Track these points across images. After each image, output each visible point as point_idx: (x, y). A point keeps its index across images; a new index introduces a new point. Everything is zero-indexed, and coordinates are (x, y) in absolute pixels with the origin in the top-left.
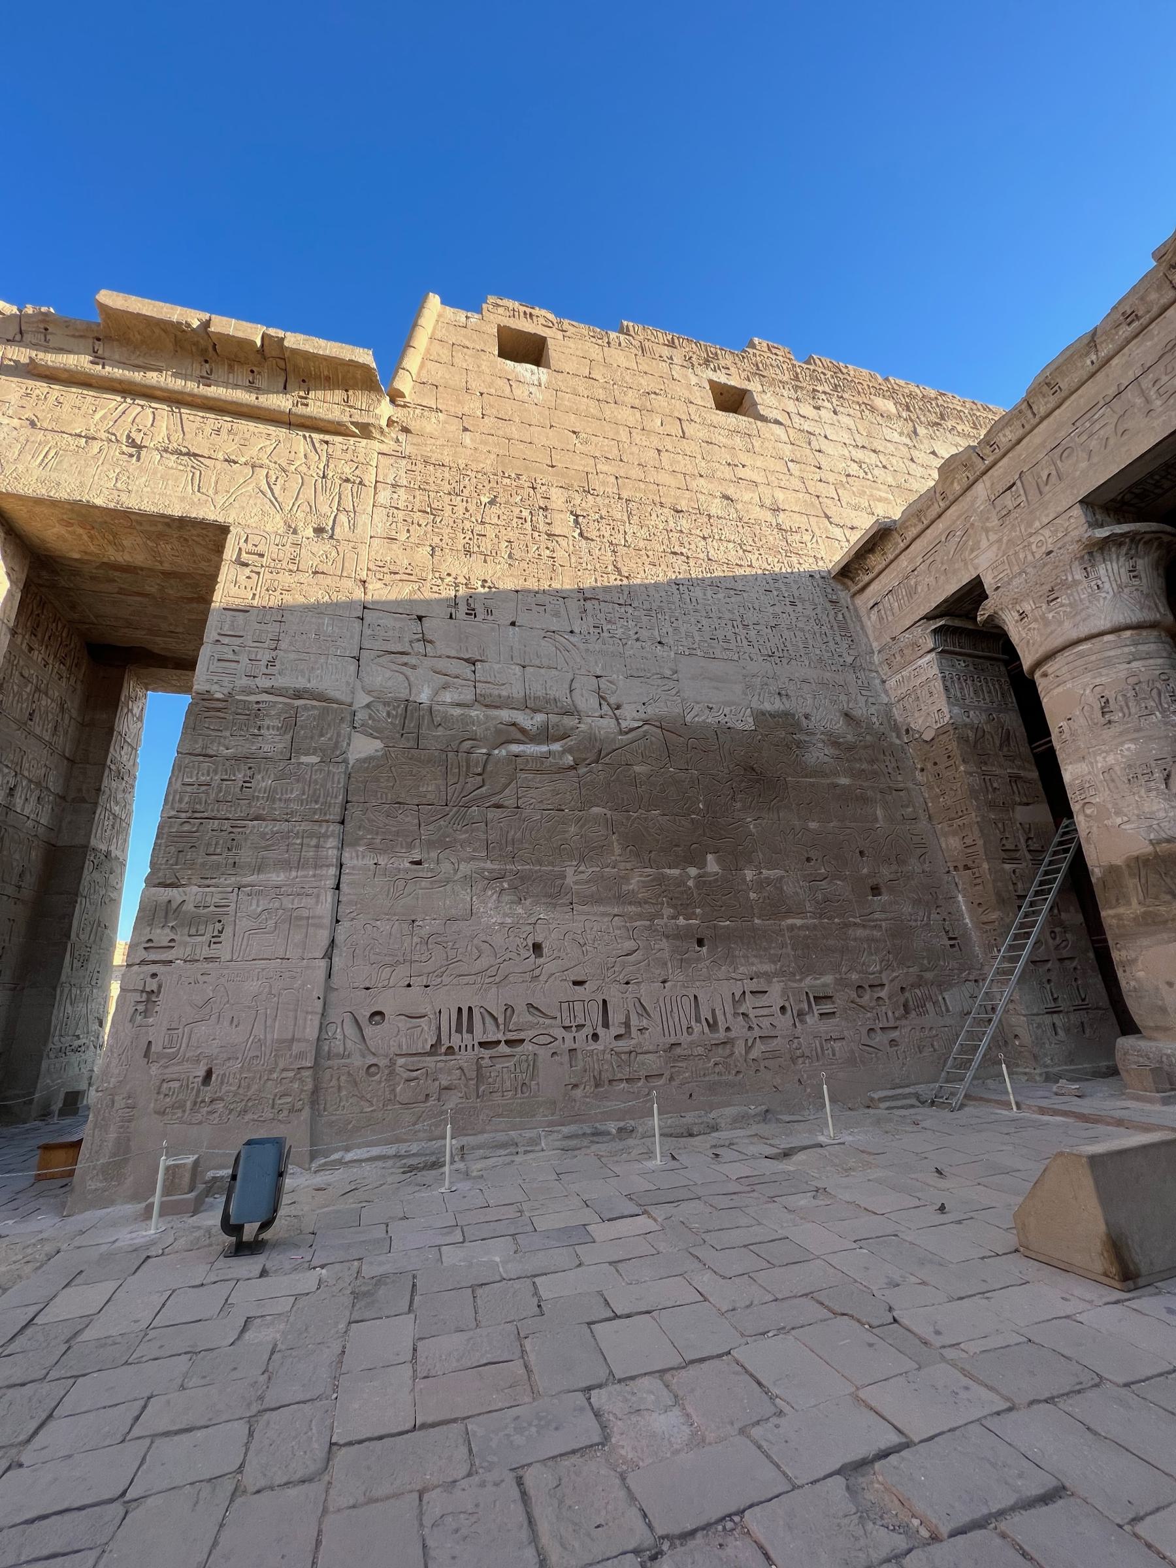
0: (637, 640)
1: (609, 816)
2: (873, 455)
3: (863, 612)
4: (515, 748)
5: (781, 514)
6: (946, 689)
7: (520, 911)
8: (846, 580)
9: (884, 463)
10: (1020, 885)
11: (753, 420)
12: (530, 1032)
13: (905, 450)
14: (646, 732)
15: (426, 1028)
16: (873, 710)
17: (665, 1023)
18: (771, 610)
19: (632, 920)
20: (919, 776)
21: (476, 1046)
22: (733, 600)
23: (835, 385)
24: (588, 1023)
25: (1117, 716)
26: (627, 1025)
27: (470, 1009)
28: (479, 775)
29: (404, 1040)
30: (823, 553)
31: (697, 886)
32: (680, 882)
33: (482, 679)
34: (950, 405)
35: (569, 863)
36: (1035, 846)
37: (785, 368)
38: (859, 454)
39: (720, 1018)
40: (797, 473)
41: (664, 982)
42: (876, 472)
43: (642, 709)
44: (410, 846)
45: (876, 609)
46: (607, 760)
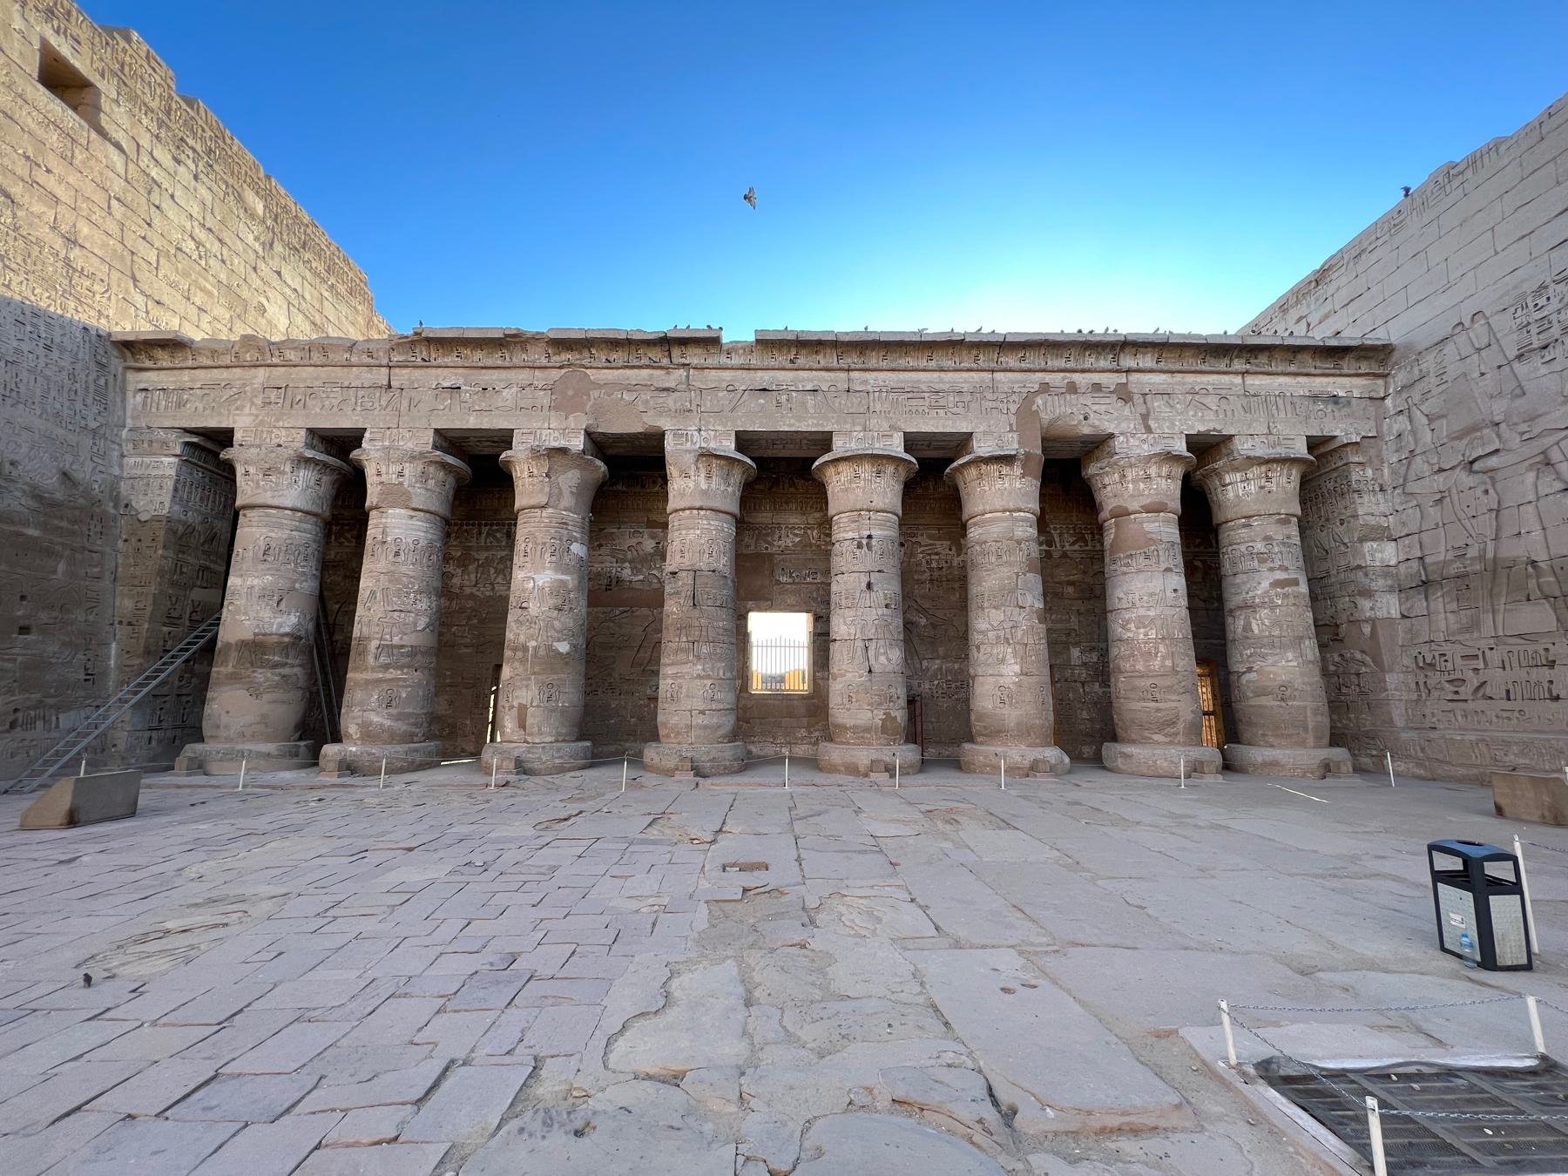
2: (217, 244)
3: (131, 387)
5: (77, 250)
6: (176, 490)
8: (126, 351)
9: (225, 258)
10: (170, 642)
11: (86, 125)
13: (253, 256)
16: (99, 477)
18: (15, 344)
20: (120, 543)
23: (211, 150)
30: (111, 312)
34: (316, 239)
36: (195, 617)
37: (158, 92)
38: (202, 235)
40: (118, 216)
42: (212, 262)
45: (144, 393)
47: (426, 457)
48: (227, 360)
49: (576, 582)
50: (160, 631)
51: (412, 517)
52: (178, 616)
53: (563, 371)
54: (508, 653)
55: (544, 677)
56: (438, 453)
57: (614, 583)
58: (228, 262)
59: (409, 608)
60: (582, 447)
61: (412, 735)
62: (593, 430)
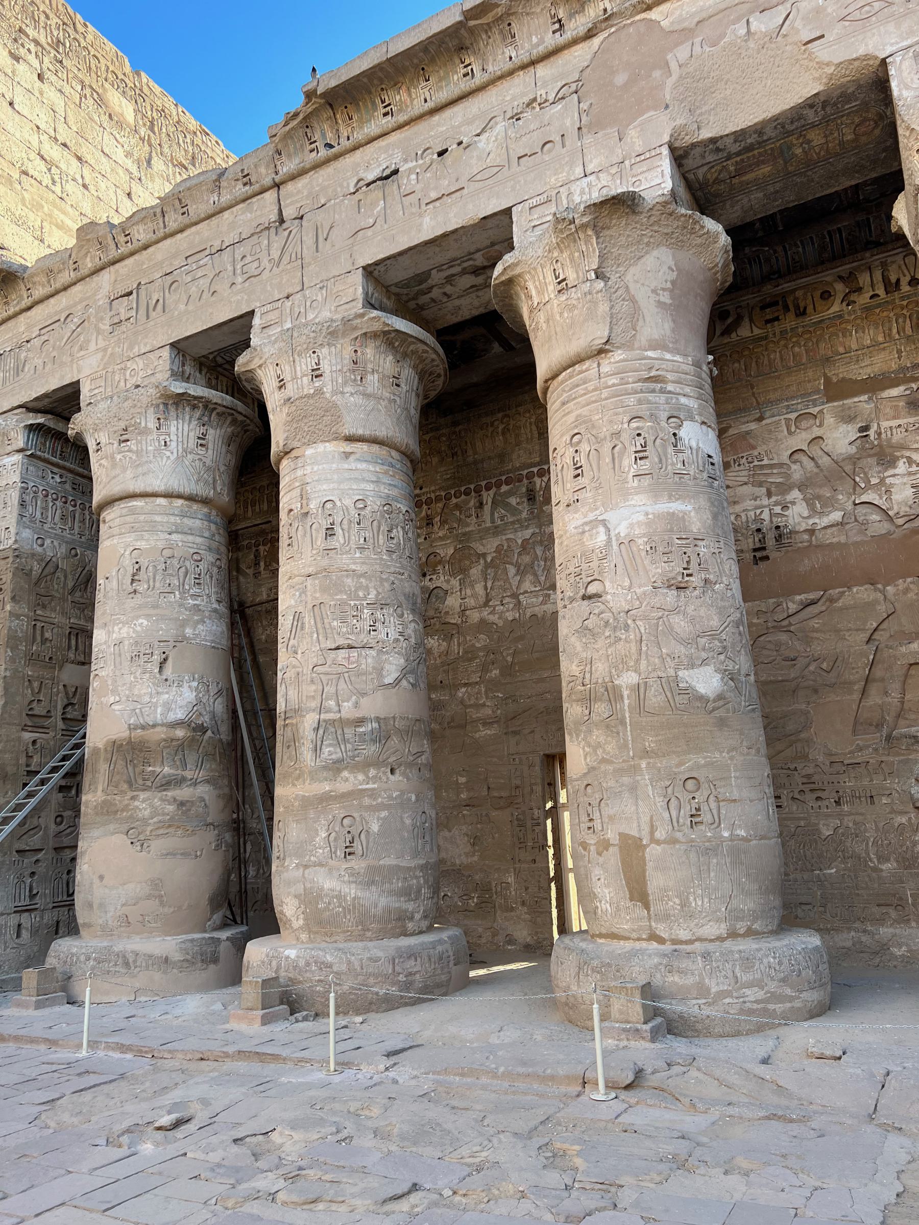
6: (22, 504)
9: (87, 182)
10: (36, 759)
25: (142, 587)
38: (54, 152)
42: (70, 187)
47: (355, 328)
48: (66, 277)
49: (707, 516)
50: (19, 739)
51: (347, 455)
52: (44, 713)
53: (596, 41)
54: (572, 711)
55: (674, 761)
56: (375, 313)
57: (770, 542)
58: (91, 187)
59: (364, 638)
60: (668, 185)
61: (402, 917)
62: (688, 140)
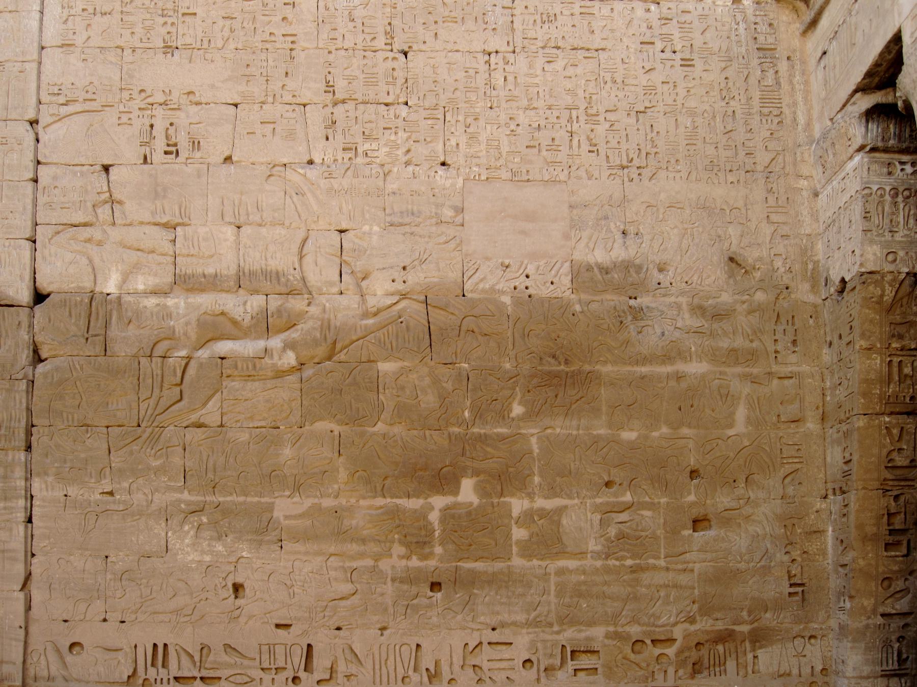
0: (407, 164)
1: (336, 433)
4: (224, 347)
7: (220, 548)
12: (226, 671)
14: (404, 309)
15: (123, 661)
17: (377, 671)
19: (352, 558)
21: (172, 680)
22: (579, 70)
24: (289, 666)
26: (332, 670)
27: (165, 645)
28: (176, 385)
29: (102, 669)
31: (443, 520)
32: (421, 515)
33: (185, 251)
35: (281, 493)
39: (445, 669)
41: (383, 629)
43: (399, 275)
44: (101, 474)
46: (342, 356)
